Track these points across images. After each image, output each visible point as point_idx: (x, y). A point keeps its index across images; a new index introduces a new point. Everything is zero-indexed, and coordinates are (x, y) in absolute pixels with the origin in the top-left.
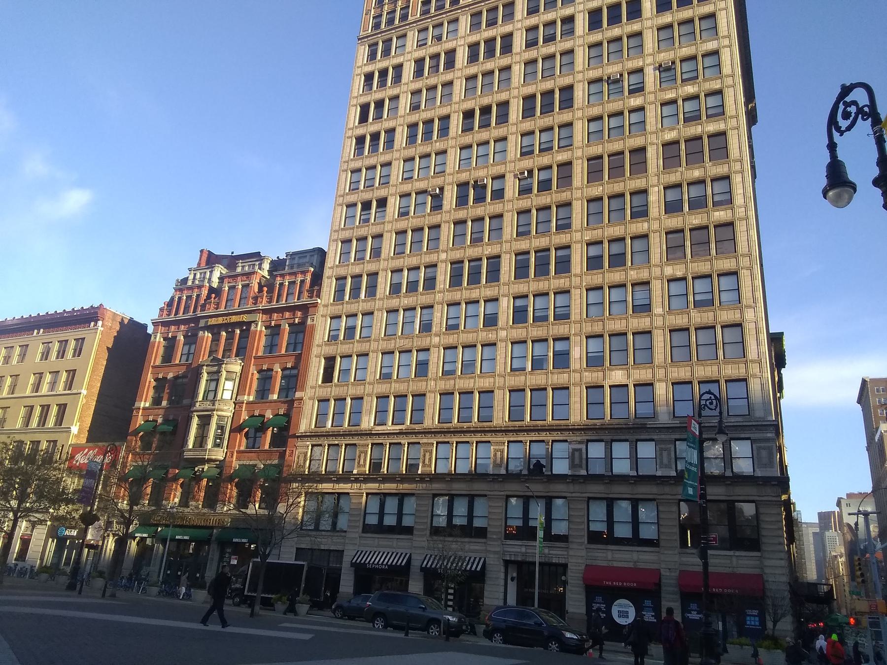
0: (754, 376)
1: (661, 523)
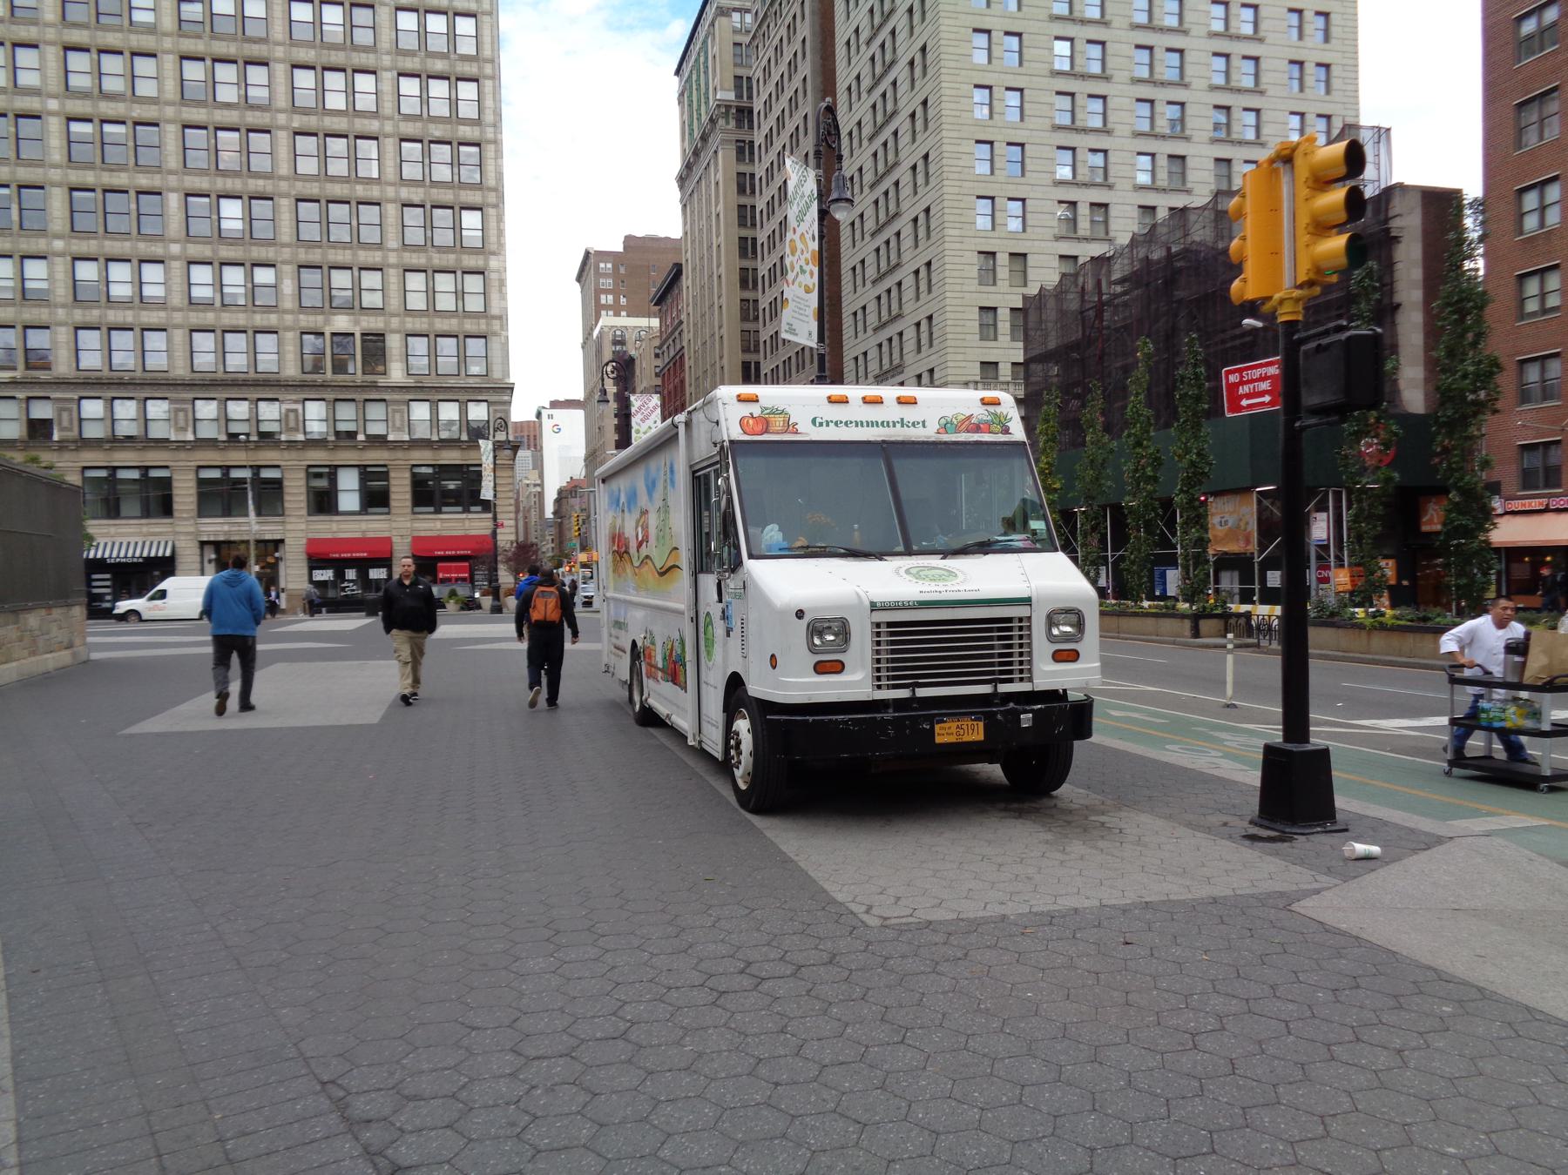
0: (495, 334)
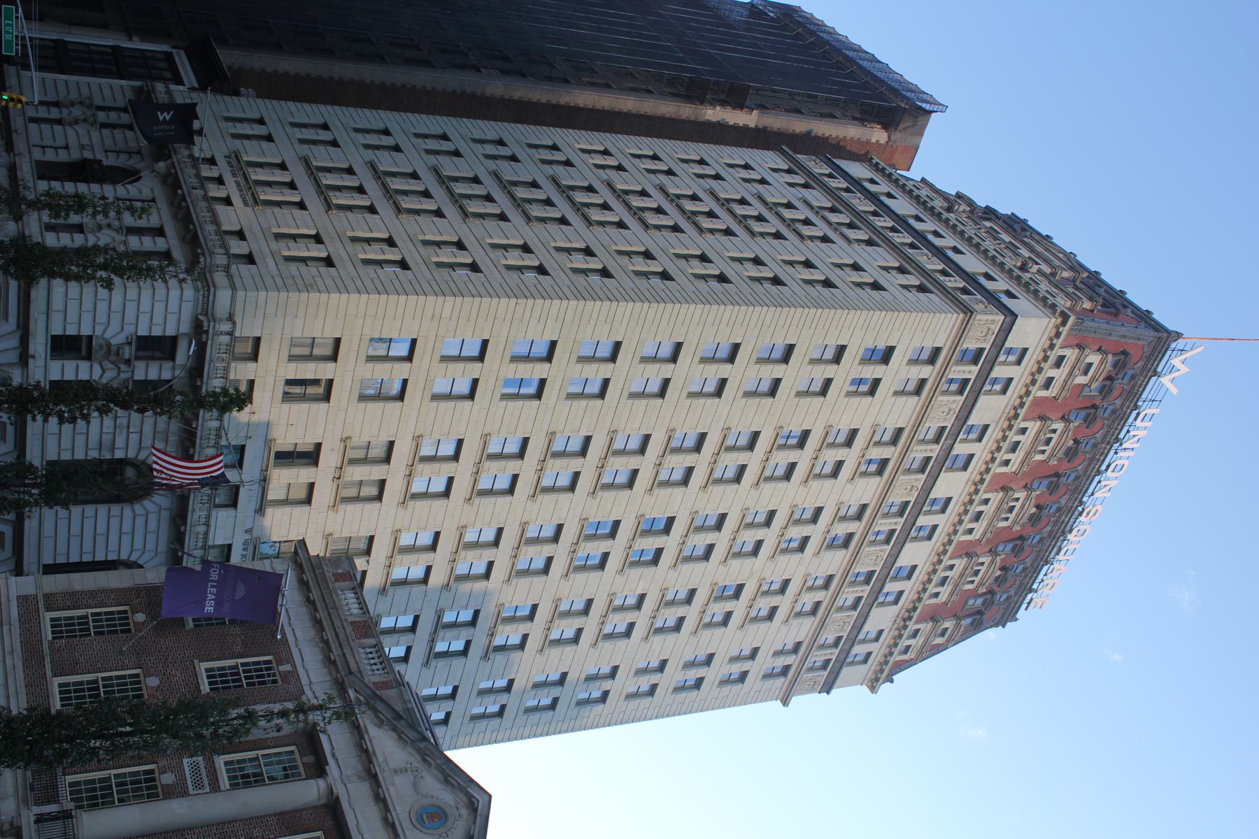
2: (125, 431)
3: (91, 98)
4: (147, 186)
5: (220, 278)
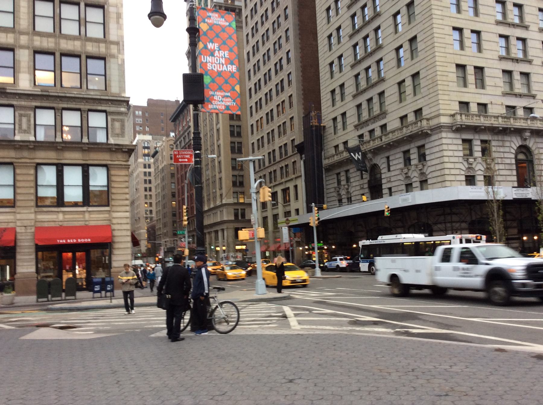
0: (113, 56)
1: (18, 184)
2: (503, 159)
3: (335, 188)
4: (380, 161)
5: (433, 123)
